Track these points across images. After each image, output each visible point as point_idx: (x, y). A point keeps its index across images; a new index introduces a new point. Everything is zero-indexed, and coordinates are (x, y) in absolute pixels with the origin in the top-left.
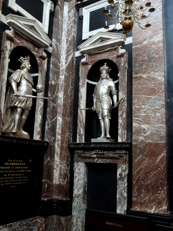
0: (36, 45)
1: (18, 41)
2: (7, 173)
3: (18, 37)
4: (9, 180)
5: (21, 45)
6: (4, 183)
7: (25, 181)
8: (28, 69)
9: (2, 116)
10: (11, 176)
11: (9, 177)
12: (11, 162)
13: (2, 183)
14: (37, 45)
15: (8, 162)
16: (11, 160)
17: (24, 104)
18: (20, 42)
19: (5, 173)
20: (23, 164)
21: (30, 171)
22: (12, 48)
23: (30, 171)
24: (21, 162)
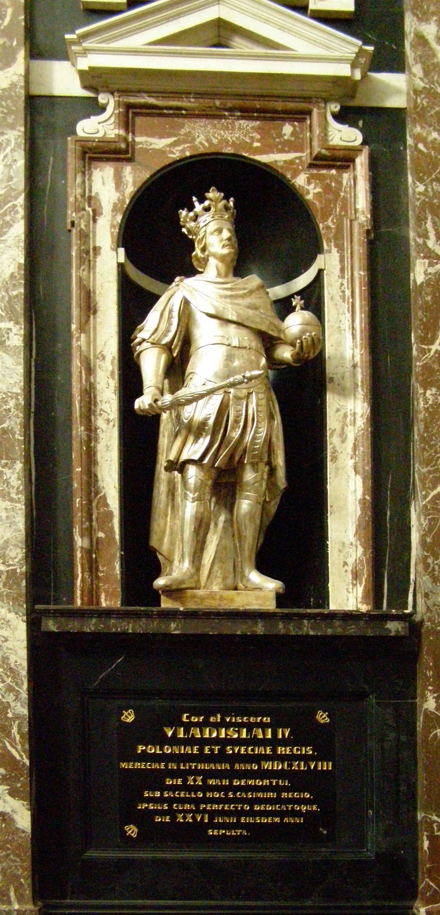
0: (275, 111)
1: (160, 143)
2: (184, 775)
3: (156, 120)
4: (197, 802)
5: (176, 154)
6: (172, 813)
7: (299, 814)
8: (222, 258)
9: (111, 521)
10: (205, 788)
11: (195, 788)
12: (201, 726)
13: (162, 813)
14: (279, 105)
15: (176, 723)
16: (198, 716)
17: (204, 442)
18: (173, 139)
19: (174, 774)
20: (275, 734)
21: (326, 766)
22: (130, 190)
23: (326, 766)
24: (263, 726)
